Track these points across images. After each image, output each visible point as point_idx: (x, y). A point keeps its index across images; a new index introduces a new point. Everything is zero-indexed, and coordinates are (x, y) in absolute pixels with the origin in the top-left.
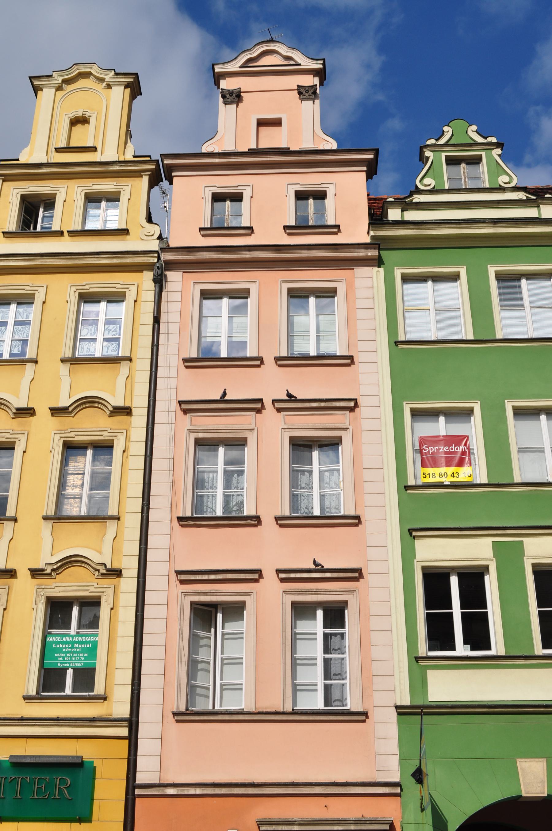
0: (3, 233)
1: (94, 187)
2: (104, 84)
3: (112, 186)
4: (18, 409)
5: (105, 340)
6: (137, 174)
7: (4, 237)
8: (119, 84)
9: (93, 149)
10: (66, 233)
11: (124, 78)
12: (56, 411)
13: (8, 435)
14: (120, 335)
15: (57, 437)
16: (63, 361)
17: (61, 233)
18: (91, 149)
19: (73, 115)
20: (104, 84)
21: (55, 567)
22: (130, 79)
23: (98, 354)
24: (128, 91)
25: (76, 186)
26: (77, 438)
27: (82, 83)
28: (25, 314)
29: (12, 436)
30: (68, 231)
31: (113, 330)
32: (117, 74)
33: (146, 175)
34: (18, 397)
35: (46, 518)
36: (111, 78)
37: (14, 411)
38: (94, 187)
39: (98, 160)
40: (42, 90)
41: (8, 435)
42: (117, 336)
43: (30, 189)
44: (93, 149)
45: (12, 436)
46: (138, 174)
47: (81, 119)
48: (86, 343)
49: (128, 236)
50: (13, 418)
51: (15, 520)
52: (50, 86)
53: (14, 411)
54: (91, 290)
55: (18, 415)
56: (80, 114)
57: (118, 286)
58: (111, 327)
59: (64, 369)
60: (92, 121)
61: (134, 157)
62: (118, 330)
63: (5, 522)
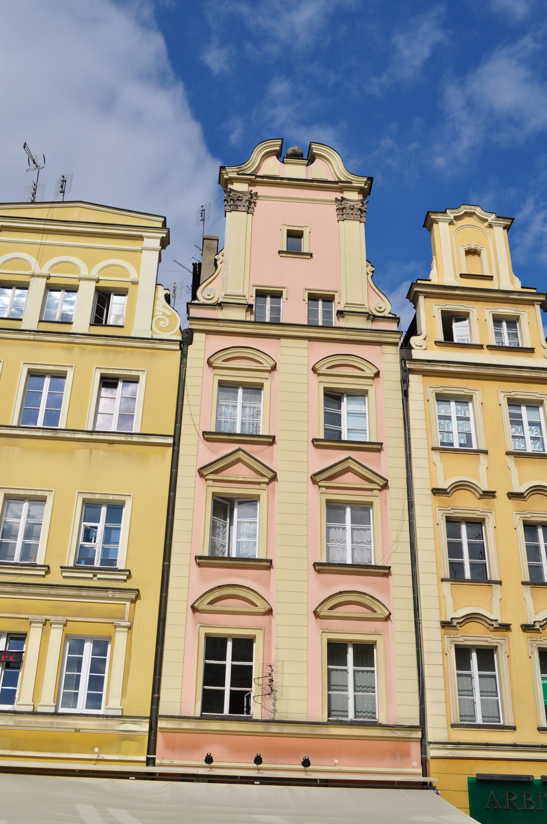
0: (435, 342)
1: (499, 310)
2: (486, 224)
3: (512, 311)
4: (484, 492)
5: (532, 438)
6: (530, 303)
7: (436, 345)
8: (499, 225)
9: (490, 278)
10: (485, 347)
11: (503, 221)
12: (512, 495)
13: (478, 513)
14: (542, 435)
15: (518, 517)
16: (508, 454)
17: (481, 347)
18: (489, 278)
19: (467, 247)
20: (486, 224)
21: (542, 624)
22: (508, 223)
23: (529, 450)
24: (506, 231)
25: (485, 308)
26: (533, 519)
27: (467, 220)
28: (463, 412)
29: (481, 513)
30: (488, 346)
31: (535, 430)
32: (498, 217)
33: (537, 304)
34: (479, 482)
35: (524, 583)
36: (493, 220)
37: (481, 493)
38: (499, 310)
39: (496, 288)
40: (437, 223)
41: (478, 513)
42: (539, 436)
43: (448, 307)
44: (490, 278)
45: (481, 513)
46: (531, 303)
47: (472, 251)
48: (516, 440)
49: (534, 354)
50: (479, 499)
51: (500, 583)
52: (444, 221)
53: (481, 493)
54: (516, 397)
55: (484, 497)
56: (473, 247)
57: (537, 395)
58: (533, 428)
59: (510, 461)
60: (483, 253)
61: (522, 287)
62: (539, 430)
63: (493, 585)
